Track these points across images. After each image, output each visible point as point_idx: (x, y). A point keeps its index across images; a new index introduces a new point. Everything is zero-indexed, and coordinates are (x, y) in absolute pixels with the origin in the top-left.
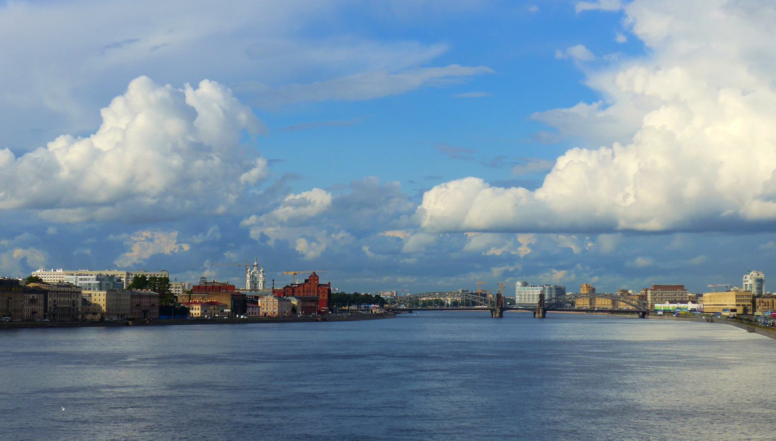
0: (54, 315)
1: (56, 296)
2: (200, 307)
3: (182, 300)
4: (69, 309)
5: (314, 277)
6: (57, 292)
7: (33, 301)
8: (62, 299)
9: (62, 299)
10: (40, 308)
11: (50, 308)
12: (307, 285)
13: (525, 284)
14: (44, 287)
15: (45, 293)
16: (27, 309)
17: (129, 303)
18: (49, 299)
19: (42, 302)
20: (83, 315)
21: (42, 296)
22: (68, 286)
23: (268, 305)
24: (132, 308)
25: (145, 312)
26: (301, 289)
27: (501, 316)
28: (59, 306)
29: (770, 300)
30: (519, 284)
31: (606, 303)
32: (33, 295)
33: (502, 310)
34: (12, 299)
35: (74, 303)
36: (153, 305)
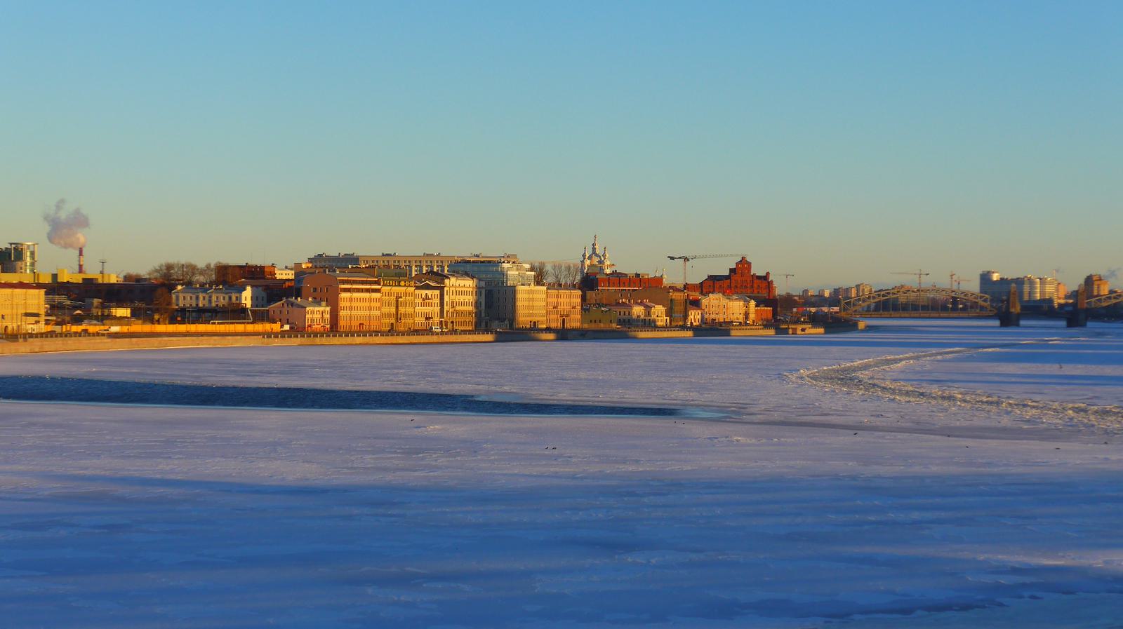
0: (452, 322)
1: (454, 294)
6: (456, 287)
8: (462, 298)
9: (462, 298)
11: (447, 311)
12: (734, 277)
17: (544, 304)
18: (446, 298)
19: (437, 301)
20: (486, 323)
21: (437, 292)
24: (547, 311)
28: (458, 308)
32: (427, 292)
34: (401, 297)
36: (574, 307)
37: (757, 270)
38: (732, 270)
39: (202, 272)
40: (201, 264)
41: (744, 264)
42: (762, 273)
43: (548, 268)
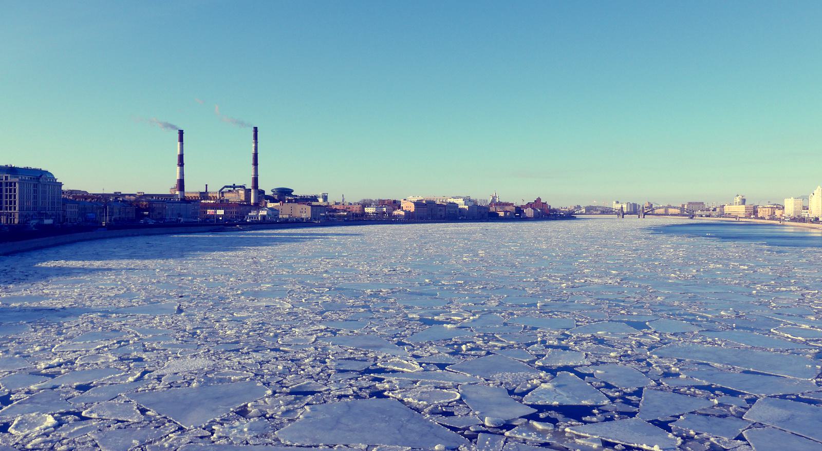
2: (503, 213)
3: (492, 209)
4: (454, 214)
5: (539, 199)
7: (440, 210)
10: (443, 214)
13: (617, 202)
14: (445, 204)
15: (445, 206)
16: (439, 213)
22: (452, 203)
23: (529, 212)
25: (483, 215)
26: (535, 204)
27: (623, 217)
28: (451, 212)
29: (768, 209)
30: (614, 202)
31: (662, 211)
33: (624, 214)
35: (456, 211)
37: (543, 201)
38: (535, 201)
39: (374, 202)
40: (374, 200)
41: (539, 199)
42: (545, 202)
43: (478, 200)
